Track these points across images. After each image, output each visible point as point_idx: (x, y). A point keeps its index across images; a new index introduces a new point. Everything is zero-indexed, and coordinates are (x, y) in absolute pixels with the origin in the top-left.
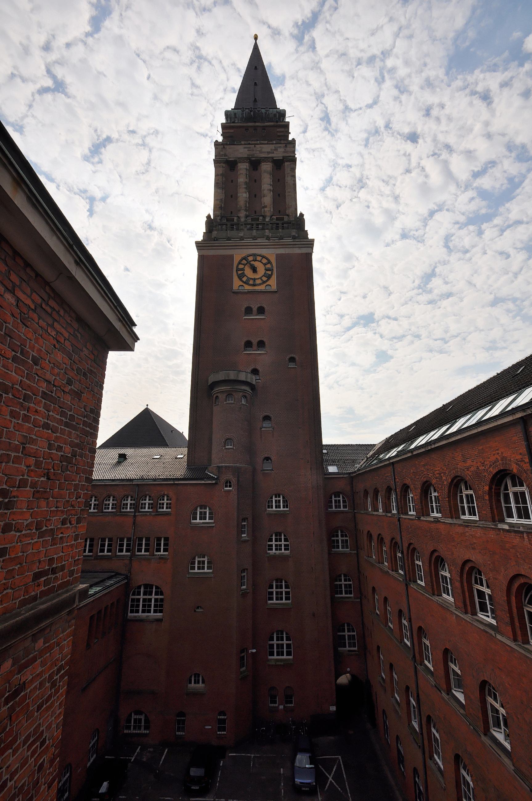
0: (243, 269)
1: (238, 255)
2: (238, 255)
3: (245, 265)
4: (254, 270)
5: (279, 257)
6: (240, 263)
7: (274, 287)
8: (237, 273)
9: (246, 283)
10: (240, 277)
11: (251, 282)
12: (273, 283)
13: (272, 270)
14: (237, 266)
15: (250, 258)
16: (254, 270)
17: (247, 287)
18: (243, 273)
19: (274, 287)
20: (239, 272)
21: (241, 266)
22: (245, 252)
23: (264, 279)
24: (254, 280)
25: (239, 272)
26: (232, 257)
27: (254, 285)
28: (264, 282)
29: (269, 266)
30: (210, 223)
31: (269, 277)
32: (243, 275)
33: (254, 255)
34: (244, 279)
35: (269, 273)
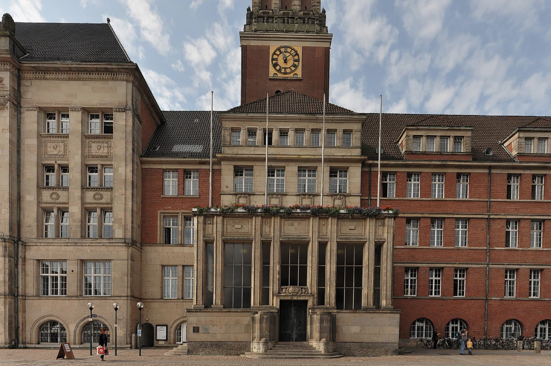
0: (276, 59)
1: (273, 46)
3: (278, 55)
4: (285, 61)
5: (304, 48)
6: (274, 54)
7: (300, 76)
8: (272, 62)
9: (279, 71)
10: (275, 65)
11: (283, 71)
12: (299, 73)
13: (298, 61)
14: (273, 56)
15: (283, 50)
17: (280, 75)
18: (277, 63)
19: (300, 76)
20: (274, 62)
21: (275, 57)
22: (278, 44)
23: (293, 68)
24: (285, 68)
25: (274, 62)
26: (268, 47)
27: (285, 73)
28: (292, 71)
29: (296, 57)
30: (250, 15)
33: (285, 47)
34: (278, 68)
35: (296, 63)
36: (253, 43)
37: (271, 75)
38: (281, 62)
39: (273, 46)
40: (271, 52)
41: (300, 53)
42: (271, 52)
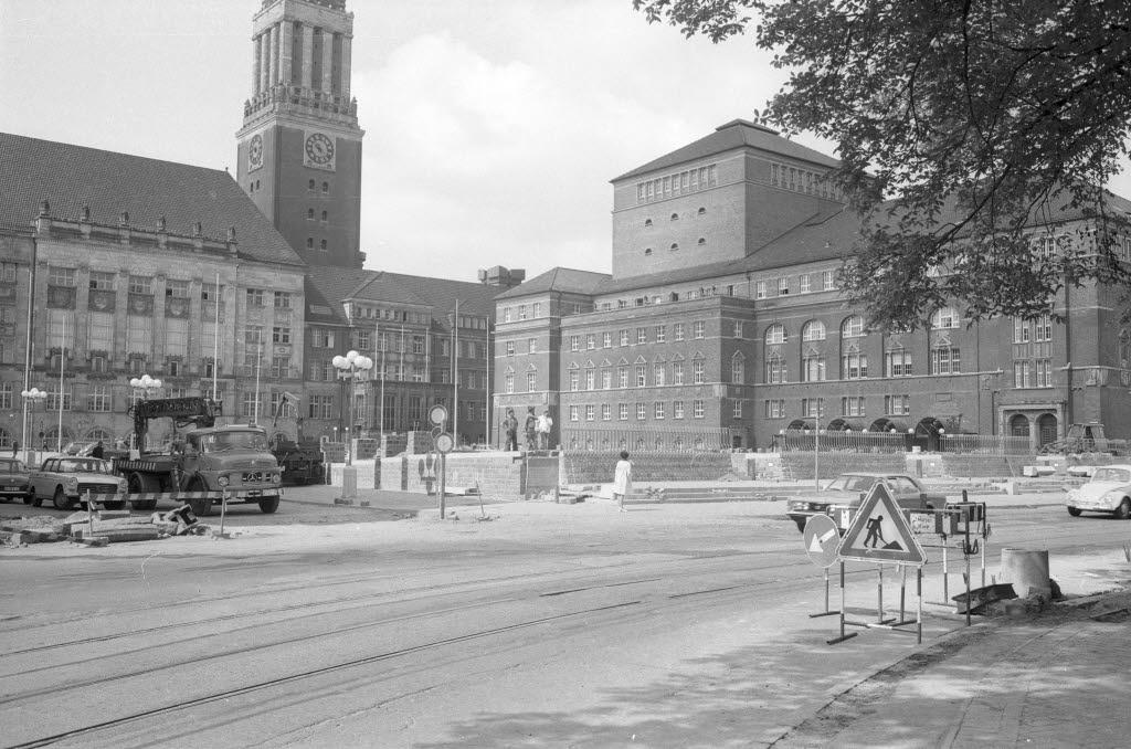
2: (309, 131)
4: (320, 149)
5: (337, 139)
9: (314, 159)
10: (309, 152)
12: (333, 162)
15: (317, 137)
16: (320, 149)
19: (334, 168)
20: (309, 149)
21: (310, 143)
27: (320, 162)
31: (329, 157)
32: (312, 152)
36: (288, 125)
37: (305, 163)
38: (315, 150)
39: (309, 131)
40: (305, 139)
41: (334, 142)
42: (305, 139)
